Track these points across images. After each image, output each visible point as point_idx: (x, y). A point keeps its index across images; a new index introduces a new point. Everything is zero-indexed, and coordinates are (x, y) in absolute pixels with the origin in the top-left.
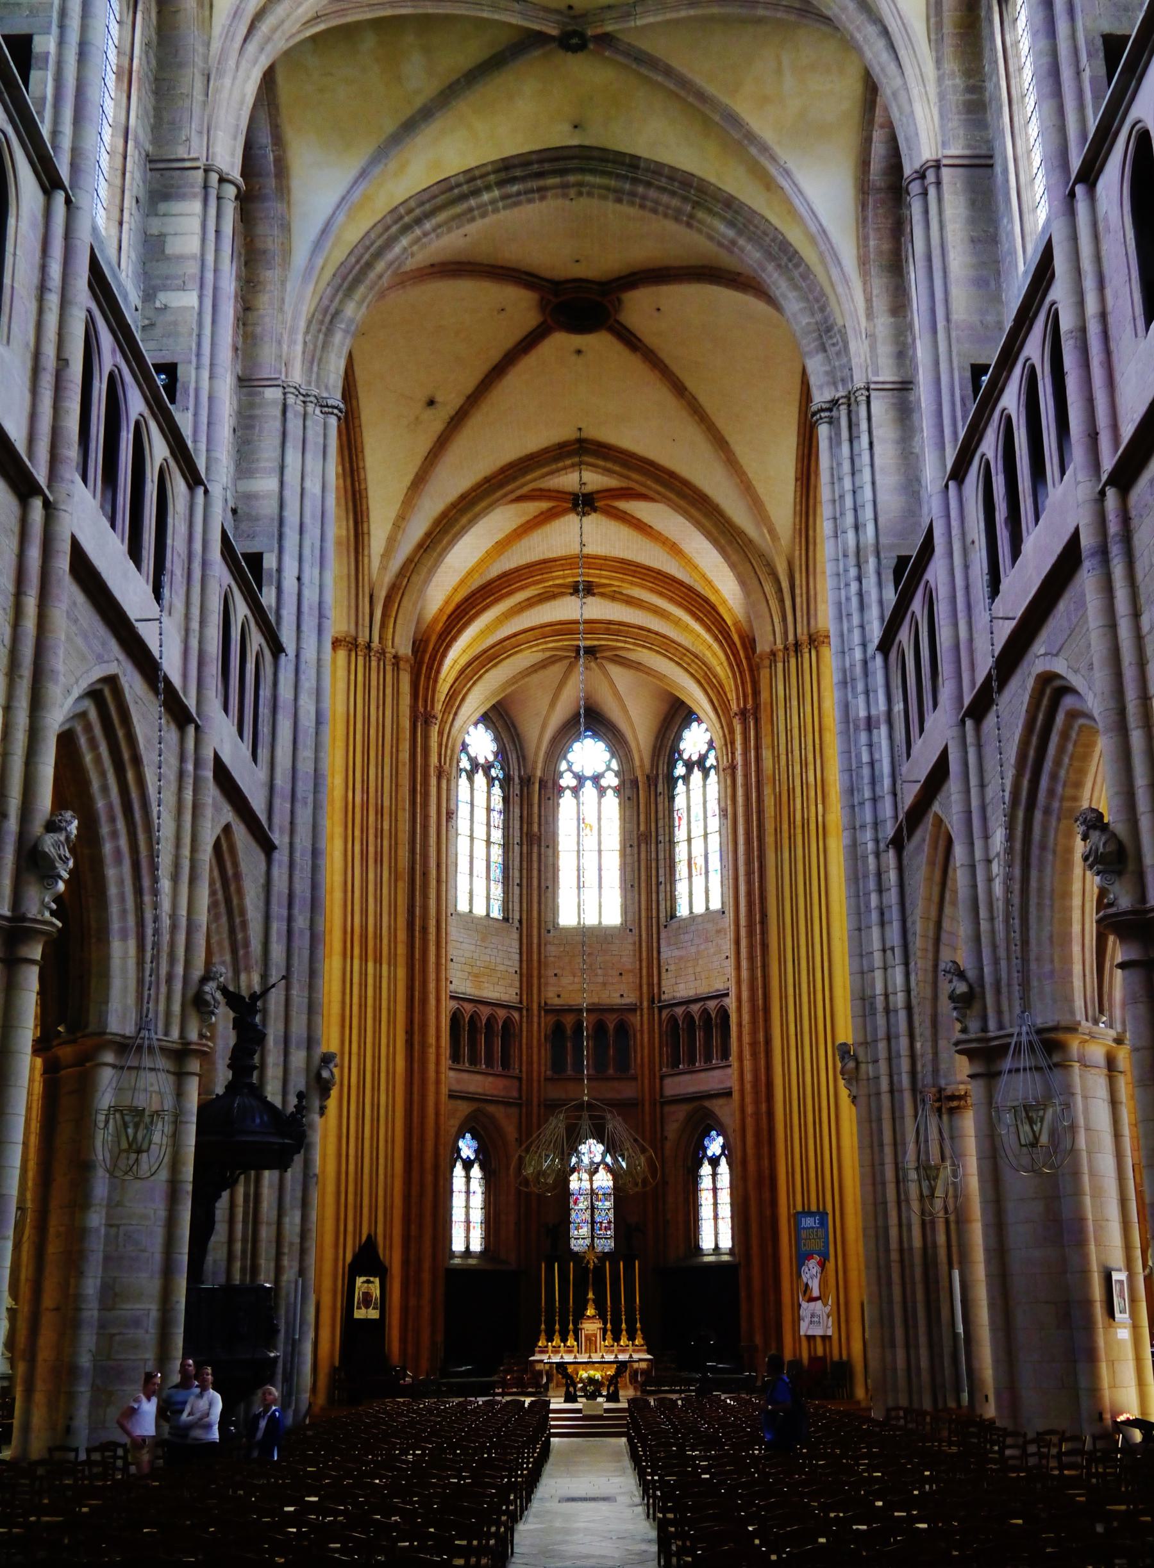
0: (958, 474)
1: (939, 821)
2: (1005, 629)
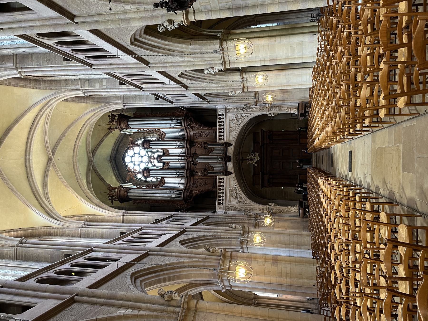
0: (141, 88)
1: (205, 95)
2: (172, 82)
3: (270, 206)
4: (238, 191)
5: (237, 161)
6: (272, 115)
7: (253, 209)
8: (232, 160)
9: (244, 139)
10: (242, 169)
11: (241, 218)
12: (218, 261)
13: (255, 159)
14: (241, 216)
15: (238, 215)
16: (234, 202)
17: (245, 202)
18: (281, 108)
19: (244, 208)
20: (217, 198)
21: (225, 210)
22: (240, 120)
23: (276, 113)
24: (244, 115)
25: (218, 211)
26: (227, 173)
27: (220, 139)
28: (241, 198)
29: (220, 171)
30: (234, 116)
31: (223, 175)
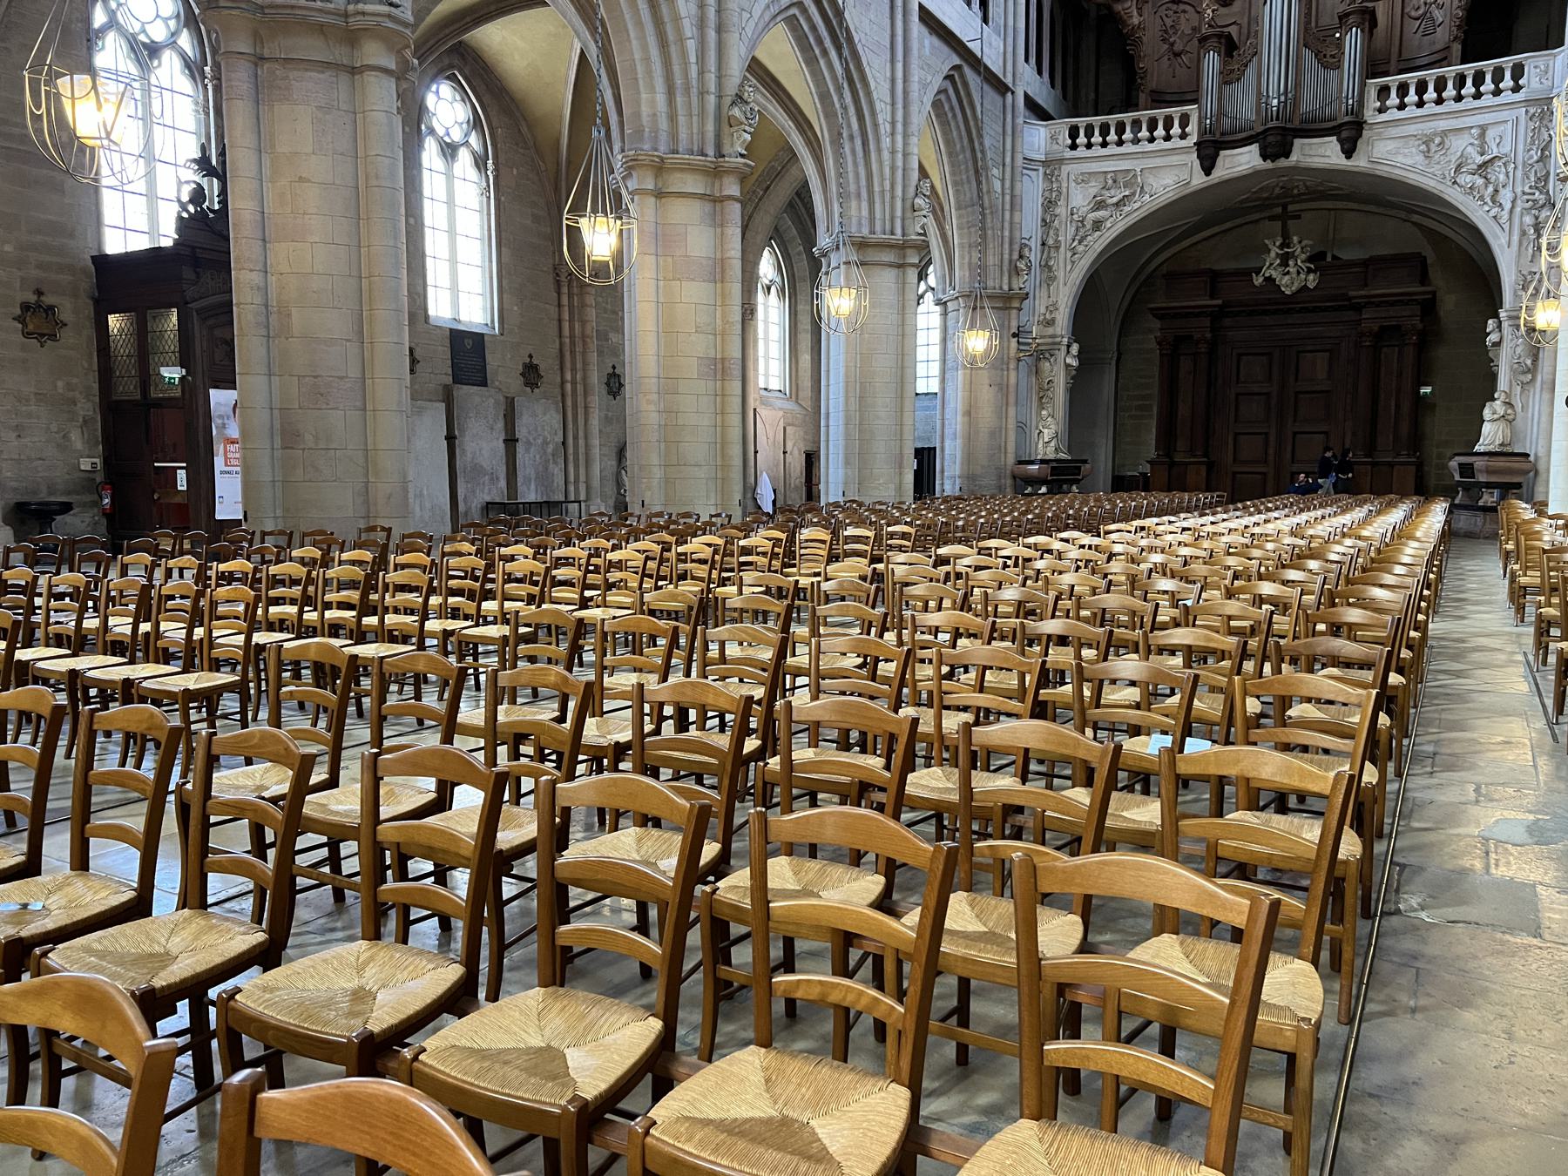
3: (1064, 348)
4: (1126, 209)
5: (1277, 191)
6: (1493, 337)
7: (1051, 279)
8: (1269, 165)
9: (1403, 215)
10: (1257, 221)
11: (1007, 233)
12: (695, 148)
13: (1288, 273)
14: (1017, 235)
15: (1017, 219)
16: (1080, 198)
17: (1080, 243)
18: (1522, 378)
19: (1057, 241)
20: (1097, 120)
21: (1045, 163)
22: (1480, 181)
23: (1497, 356)
24: (1506, 197)
25: (1042, 130)
26: (1208, 153)
27: (1384, 91)
28: (1097, 225)
29: (1221, 113)
30: (1506, 148)
31: (1202, 131)
